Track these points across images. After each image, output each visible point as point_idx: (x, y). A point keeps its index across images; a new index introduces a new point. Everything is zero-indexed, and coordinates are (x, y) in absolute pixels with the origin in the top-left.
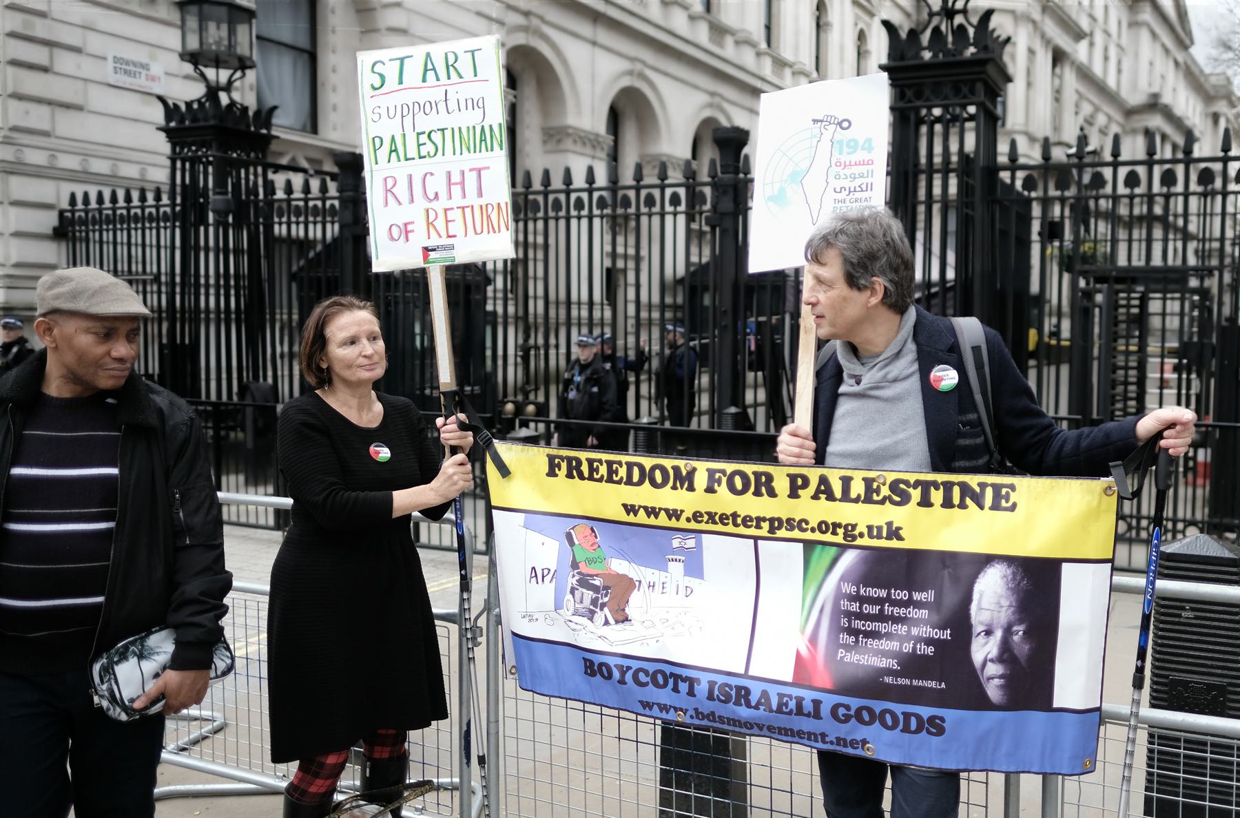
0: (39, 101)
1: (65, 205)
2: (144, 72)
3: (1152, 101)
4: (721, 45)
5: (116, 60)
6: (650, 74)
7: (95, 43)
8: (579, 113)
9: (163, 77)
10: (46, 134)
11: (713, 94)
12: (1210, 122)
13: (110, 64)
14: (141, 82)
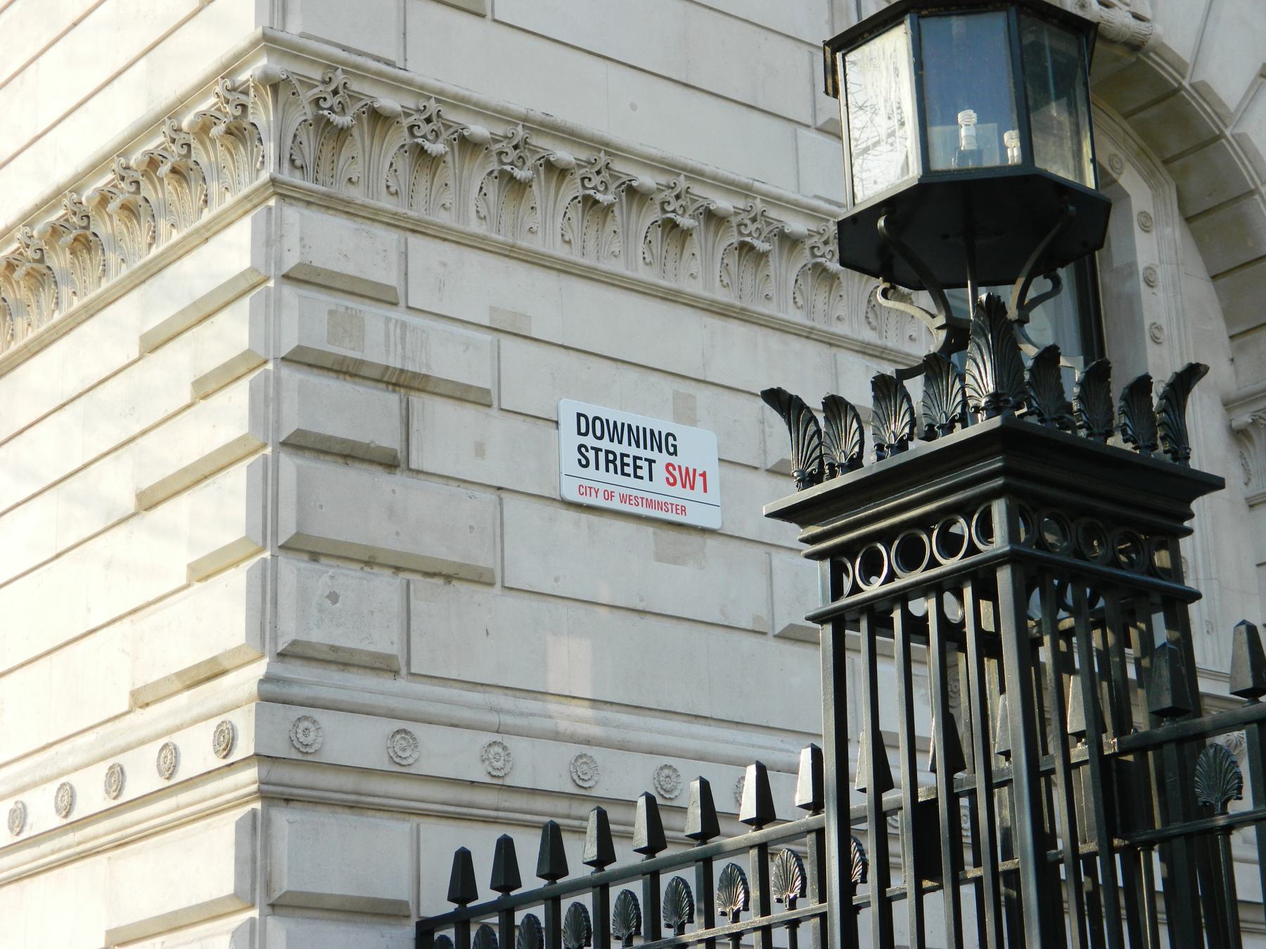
0: (369, 560)
1: (438, 903)
2: (662, 459)
5: (586, 424)
7: (525, 376)
9: (715, 473)
10: (384, 666)
13: (569, 438)
14: (656, 488)
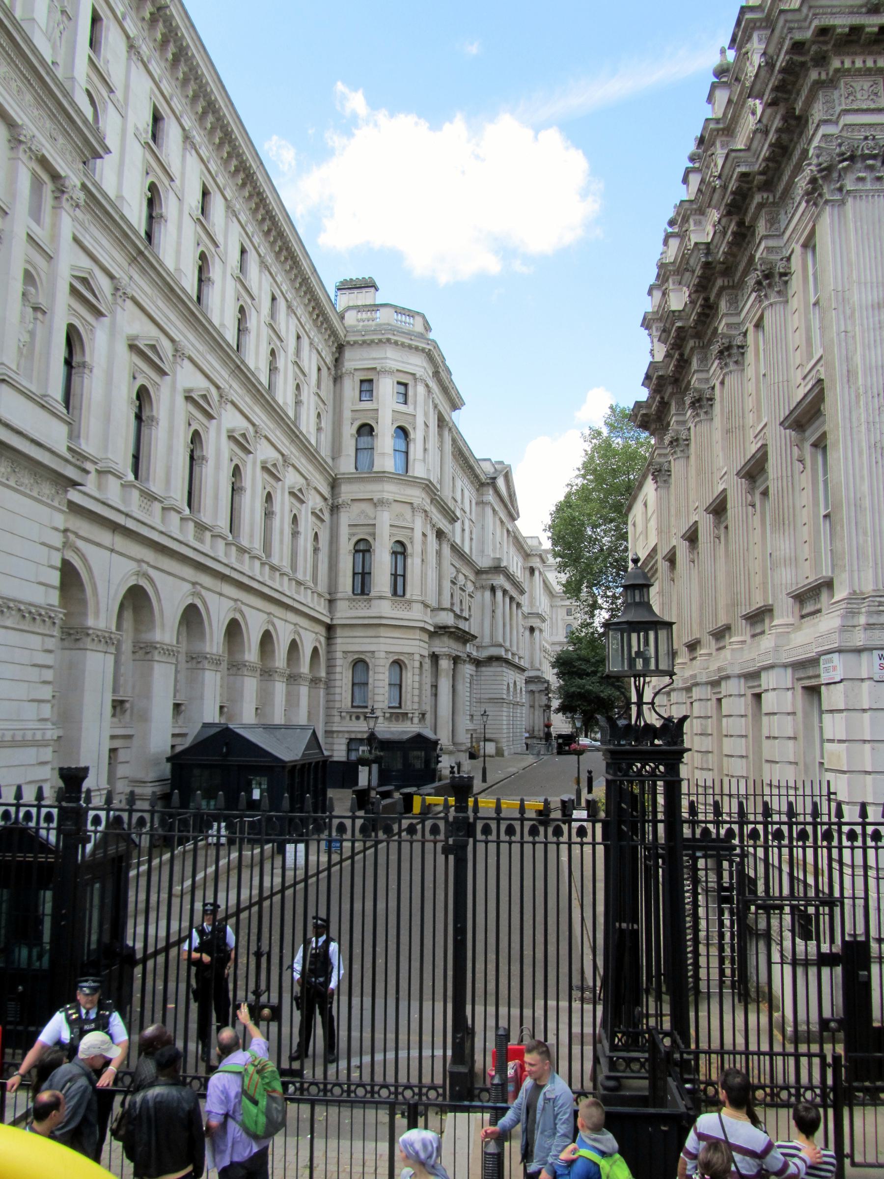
3: (496, 564)
4: (201, 541)
6: (152, 572)
8: (97, 614)
11: (194, 584)
12: (527, 573)
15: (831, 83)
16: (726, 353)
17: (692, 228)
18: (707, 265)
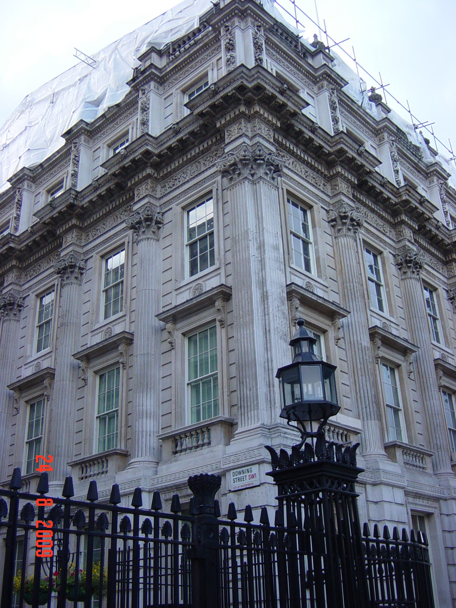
15: (249, 118)
16: (69, 270)
17: (26, 187)
18: (71, 206)
